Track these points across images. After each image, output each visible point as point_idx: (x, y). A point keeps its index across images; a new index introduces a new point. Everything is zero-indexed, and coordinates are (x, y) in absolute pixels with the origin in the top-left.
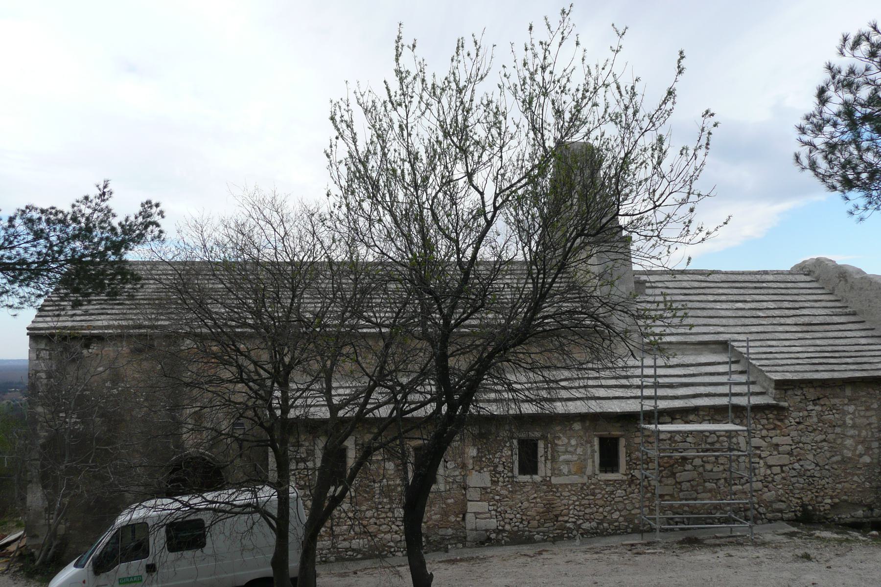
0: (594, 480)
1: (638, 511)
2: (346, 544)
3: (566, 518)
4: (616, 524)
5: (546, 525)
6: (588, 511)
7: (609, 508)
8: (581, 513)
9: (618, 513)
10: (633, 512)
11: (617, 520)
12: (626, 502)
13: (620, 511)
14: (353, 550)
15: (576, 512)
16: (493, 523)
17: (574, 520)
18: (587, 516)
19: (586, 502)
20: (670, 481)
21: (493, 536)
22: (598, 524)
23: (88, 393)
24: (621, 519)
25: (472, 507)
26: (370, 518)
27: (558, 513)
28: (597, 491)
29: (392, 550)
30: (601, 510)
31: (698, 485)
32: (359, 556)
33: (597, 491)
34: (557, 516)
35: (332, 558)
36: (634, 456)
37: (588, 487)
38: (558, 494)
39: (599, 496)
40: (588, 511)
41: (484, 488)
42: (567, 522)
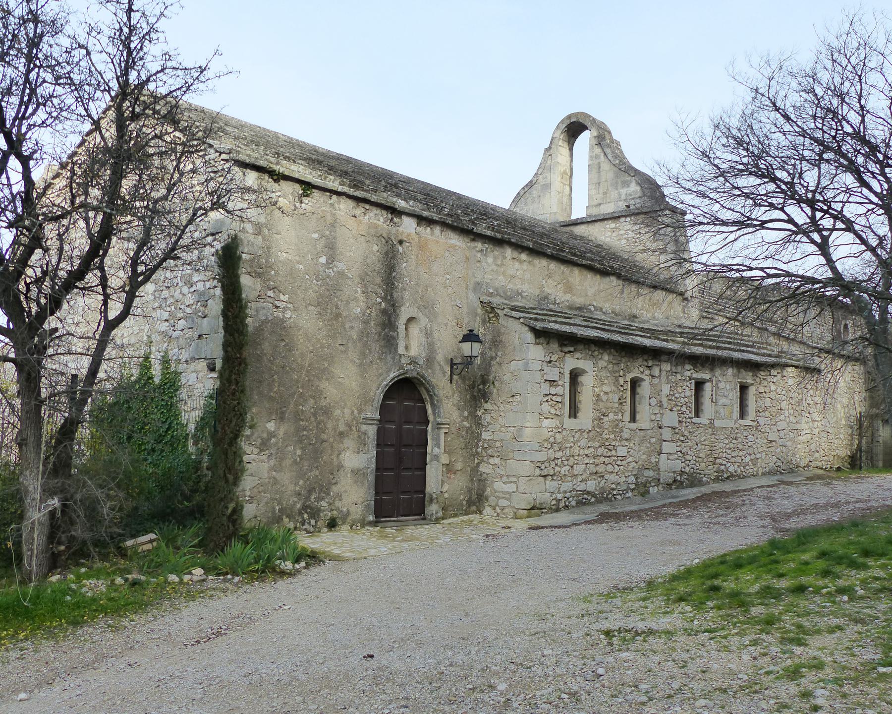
3: (721, 461)
6: (733, 454)
13: (750, 455)
14: (588, 493)
16: (678, 466)
18: (733, 460)
19: (732, 446)
21: (678, 478)
23: (301, 267)
25: (667, 447)
27: (716, 455)
32: (593, 500)
35: (574, 503)
41: (674, 428)
42: (721, 464)
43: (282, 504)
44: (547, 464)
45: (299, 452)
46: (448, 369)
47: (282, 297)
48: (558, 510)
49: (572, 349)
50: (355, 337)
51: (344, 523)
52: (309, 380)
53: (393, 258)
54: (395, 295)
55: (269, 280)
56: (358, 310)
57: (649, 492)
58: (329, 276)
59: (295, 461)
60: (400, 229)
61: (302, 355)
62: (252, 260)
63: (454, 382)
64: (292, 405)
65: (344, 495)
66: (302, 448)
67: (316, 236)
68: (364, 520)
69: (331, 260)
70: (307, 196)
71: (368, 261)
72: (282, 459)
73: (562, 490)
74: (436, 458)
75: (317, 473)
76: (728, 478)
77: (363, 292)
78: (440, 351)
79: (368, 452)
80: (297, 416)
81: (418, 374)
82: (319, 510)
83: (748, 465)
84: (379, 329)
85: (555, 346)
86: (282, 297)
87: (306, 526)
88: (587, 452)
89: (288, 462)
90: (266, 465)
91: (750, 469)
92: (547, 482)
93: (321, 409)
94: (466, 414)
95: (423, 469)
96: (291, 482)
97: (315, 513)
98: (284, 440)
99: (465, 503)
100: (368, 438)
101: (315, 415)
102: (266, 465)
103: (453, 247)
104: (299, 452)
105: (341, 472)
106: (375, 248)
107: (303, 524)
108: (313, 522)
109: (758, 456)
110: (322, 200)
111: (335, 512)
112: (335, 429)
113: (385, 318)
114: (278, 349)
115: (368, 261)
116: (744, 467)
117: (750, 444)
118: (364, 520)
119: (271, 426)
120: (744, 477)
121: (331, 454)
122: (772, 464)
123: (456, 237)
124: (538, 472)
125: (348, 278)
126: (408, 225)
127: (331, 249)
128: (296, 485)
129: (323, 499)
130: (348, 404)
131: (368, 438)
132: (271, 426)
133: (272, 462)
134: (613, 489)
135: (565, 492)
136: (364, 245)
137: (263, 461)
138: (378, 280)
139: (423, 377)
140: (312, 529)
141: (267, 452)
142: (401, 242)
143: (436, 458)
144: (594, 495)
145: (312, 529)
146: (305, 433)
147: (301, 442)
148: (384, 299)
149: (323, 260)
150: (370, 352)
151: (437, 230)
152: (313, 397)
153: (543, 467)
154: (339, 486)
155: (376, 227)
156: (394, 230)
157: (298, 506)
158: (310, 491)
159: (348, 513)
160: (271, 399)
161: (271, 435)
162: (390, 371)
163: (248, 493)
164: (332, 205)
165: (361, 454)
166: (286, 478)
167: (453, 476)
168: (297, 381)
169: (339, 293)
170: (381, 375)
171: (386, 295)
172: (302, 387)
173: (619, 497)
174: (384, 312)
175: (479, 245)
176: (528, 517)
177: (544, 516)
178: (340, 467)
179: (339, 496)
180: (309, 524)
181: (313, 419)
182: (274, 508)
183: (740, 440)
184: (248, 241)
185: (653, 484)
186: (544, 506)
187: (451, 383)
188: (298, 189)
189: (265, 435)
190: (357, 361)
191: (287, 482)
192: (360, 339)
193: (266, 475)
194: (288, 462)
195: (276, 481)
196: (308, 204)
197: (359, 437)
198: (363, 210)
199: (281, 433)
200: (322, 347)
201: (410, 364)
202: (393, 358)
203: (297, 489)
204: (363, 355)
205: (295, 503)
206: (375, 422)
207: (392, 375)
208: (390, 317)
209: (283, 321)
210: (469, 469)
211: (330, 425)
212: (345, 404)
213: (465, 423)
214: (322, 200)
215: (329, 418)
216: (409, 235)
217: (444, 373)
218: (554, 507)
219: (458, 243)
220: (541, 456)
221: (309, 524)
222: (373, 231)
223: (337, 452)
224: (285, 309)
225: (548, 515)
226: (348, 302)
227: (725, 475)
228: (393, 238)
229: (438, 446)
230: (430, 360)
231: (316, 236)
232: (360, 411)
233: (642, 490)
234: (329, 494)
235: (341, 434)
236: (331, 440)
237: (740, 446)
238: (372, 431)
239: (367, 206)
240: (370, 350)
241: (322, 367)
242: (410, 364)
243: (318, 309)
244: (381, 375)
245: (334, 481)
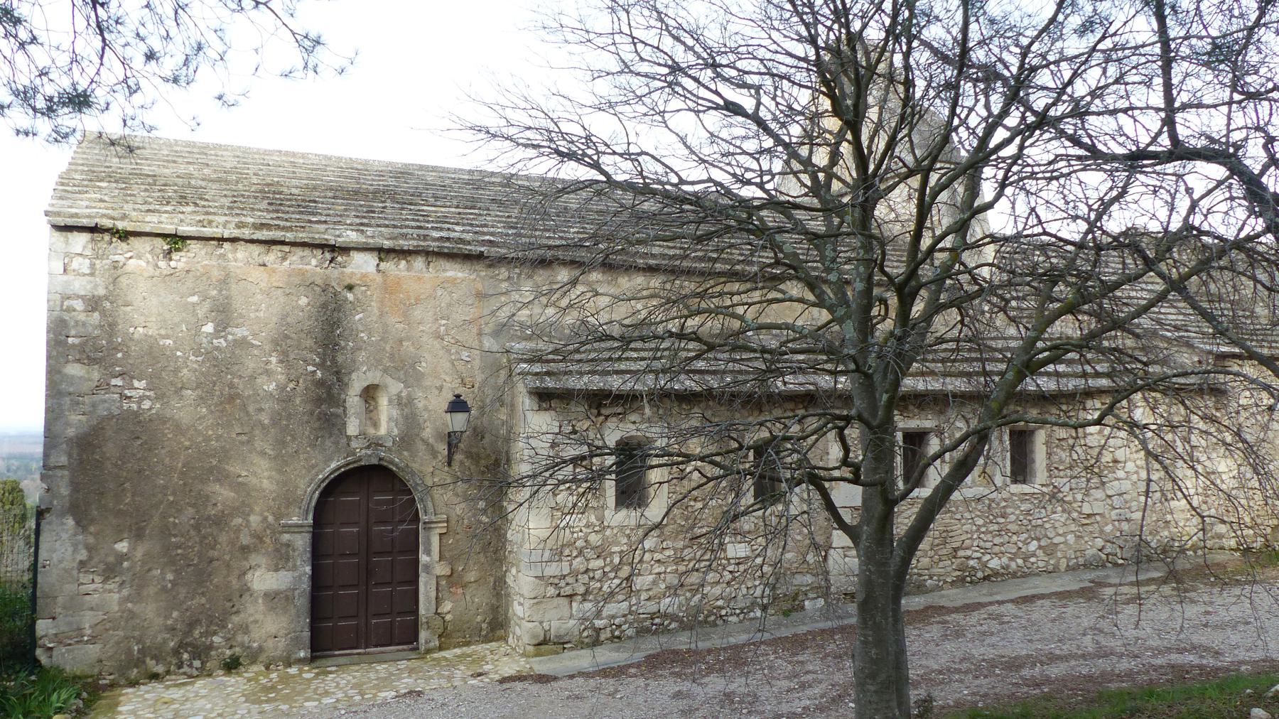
0: (1005, 495)
1: (1061, 539)
2: (652, 607)
3: (969, 553)
4: (1033, 560)
5: (941, 564)
6: (997, 540)
7: (1025, 535)
8: (989, 545)
9: (1035, 542)
10: (1055, 541)
11: (1034, 555)
12: (1047, 526)
13: (1038, 539)
14: (666, 616)
15: (982, 544)
17: (979, 555)
18: (996, 549)
20: (1098, 494)
22: (1011, 559)
23: (169, 342)
24: (1039, 553)
26: (690, 560)
28: (1009, 510)
29: (723, 612)
30: (1015, 538)
31: (1132, 500)
32: (673, 625)
33: (1009, 510)
34: (956, 550)
35: (630, 632)
36: (1055, 458)
37: (998, 504)
38: (958, 516)
39: (1013, 518)
40: (997, 540)
42: (968, 558)
43: (144, 644)
44: (569, 580)
45: (170, 576)
46: (443, 448)
47: (136, 384)
48: (596, 643)
49: (620, 410)
50: (266, 422)
51: (253, 662)
52: (185, 484)
53: (338, 309)
54: (340, 359)
55: (113, 365)
56: (273, 386)
57: (803, 608)
58: (217, 348)
59: (164, 589)
60: (348, 270)
61: (172, 454)
62: (83, 345)
63: (456, 466)
64: (156, 519)
65: (251, 627)
66: (176, 571)
67: (195, 299)
68: (289, 657)
69: (222, 327)
70: (178, 250)
71: (289, 319)
72: (141, 587)
73: (604, 613)
74: (428, 568)
75: (203, 600)
76: (985, 578)
77: (281, 362)
78: (428, 424)
79: (294, 568)
80: (166, 531)
81: (380, 459)
82: (211, 647)
83: (1034, 555)
84: (309, 407)
85: (579, 409)
86: (136, 384)
87: (185, 669)
88: (657, 556)
89: (152, 590)
90: (116, 596)
91: (1040, 561)
92: (574, 604)
93: (209, 518)
94: (482, 504)
95: (415, 581)
96: (159, 615)
97: (200, 652)
98: (144, 563)
99: (484, 626)
100: (294, 550)
101: (197, 527)
102: (116, 596)
103: (453, 281)
104: (170, 576)
105: (246, 597)
106: (303, 301)
107: (180, 667)
108: (197, 663)
109: (1057, 540)
110: (203, 252)
111: (237, 649)
112: (232, 543)
113: (322, 392)
114: (129, 451)
115: (289, 319)
116: (1025, 560)
117: (1040, 522)
118: (289, 657)
119: (122, 547)
120: (1025, 575)
121: (228, 575)
122: (1090, 552)
123: (457, 266)
124: (551, 591)
125: (253, 346)
126: (363, 264)
127: (223, 314)
128: (166, 618)
129: (215, 633)
130: (257, 509)
131: (294, 550)
132: (122, 547)
133: (125, 592)
134: (721, 608)
135: (613, 617)
136: (282, 299)
137: (110, 591)
138: (309, 343)
139: (392, 462)
140: (195, 673)
141: (117, 579)
142: (350, 288)
143: (428, 568)
144: (674, 618)
145: (195, 673)
146: (179, 551)
147: (172, 562)
148: (321, 366)
149: (209, 328)
150: (294, 439)
151: (419, 263)
152: (194, 506)
153: (562, 584)
154: (242, 615)
155: (302, 273)
156: (334, 273)
157: (172, 644)
158: (192, 625)
159: (261, 649)
160: (119, 513)
161: (122, 557)
162: (331, 460)
163: (89, 632)
164: (223, 256)
165: (282, 573)
166: (149, 611)
167: (460, 591)
168: (165, 487)
169: (236, 368)
170: (313, 467)
171: (324, 362)
172: (174, 494)
173: (733, 619)
174: (320, 383)
175: (503, 272)
176: (536, 655)
177: (567, 654)
178: (245, 590)
179: (246, 629)
180: (191, 666)
181: (192, 533)
182: (130, 650)
183: (1013, 518)
184: (77, 322)
185: (811, 595)
186: (567, 639)
187: (449, 464)
188: (163, 245)
189: (111, 559)
190: (270, 452)
191: (150, 615)
192: (275, 422)
193: (116, 608)
194: (152, 590)
195: (132, 615)
196: (180, 260)
197: (277, 550)
198: (279, 254)
199: (139, 554)
200: (207, 439)
201: (368, 447)
202: (337, 443)
203: (169, 622)
204: (281, 443)
205: (165, 641)
207: (333, 465)
208: (330, 388)
209: (136, 414)
210: (492, 579)
211: (223, 538)
212: (252, 510)
213: (485, 519)
214: (203, 252)
215: (221, 530)
216: (364, 276)
217: (434, 454)
218: (586, 640)
219: (460, 275)
220: (553, 569)
221: (191, 666)
222: (297, 280)
223: (236, 572)
224: (142, 398)
225: (574, 653)
226: (253, 378)
227: (980, 575)
228: (333, 284)
229: (428, 553)
230: (407, 440)
231: (195, 299)
232: (278, 517)
233: (786, 606)
234: (224, 627)
235: (245, 550)
236: (227, 557)
237: (1013, 527)
238: (302, 542)
239: (287, 249)
240: (292, 436)
241: (208, 466)
242: (368, 447)
243: (199, 392)
244: (313, 467)
245: (235, 609)
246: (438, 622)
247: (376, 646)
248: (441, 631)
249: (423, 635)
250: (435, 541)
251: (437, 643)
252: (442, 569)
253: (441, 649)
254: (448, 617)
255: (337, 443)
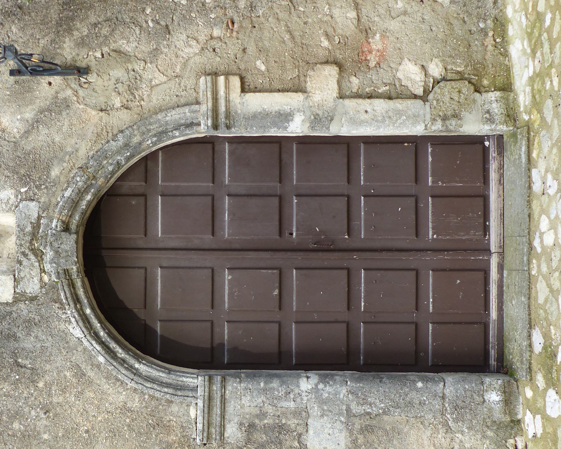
46: (47, 87)
68: (499, 426)
74: (316, 120)
79: (302, 414)
81: (66, 229)
95: (348, 145)
100: (262, 415)
118: (499, 426)
131: (262, 415)
139: (74, 204)
150: (17, 415)
162: (64, 336)
167: (376, 42)
170: (80, 374)
201: (39, 255)
202: (29, 324)
206: (216, 387)
217: (59, 106)
229: (285, 117)
242: (39, 255)
244: (80, 374)
246: (445, 92)
247: (486, 229)
248: (466, 87)
249: (472, 126)
250: (256, 102)
251: (493, 95)
252: (324, 85)
253: (506, 87)
254: (436, 70)
255: (29, 324)
